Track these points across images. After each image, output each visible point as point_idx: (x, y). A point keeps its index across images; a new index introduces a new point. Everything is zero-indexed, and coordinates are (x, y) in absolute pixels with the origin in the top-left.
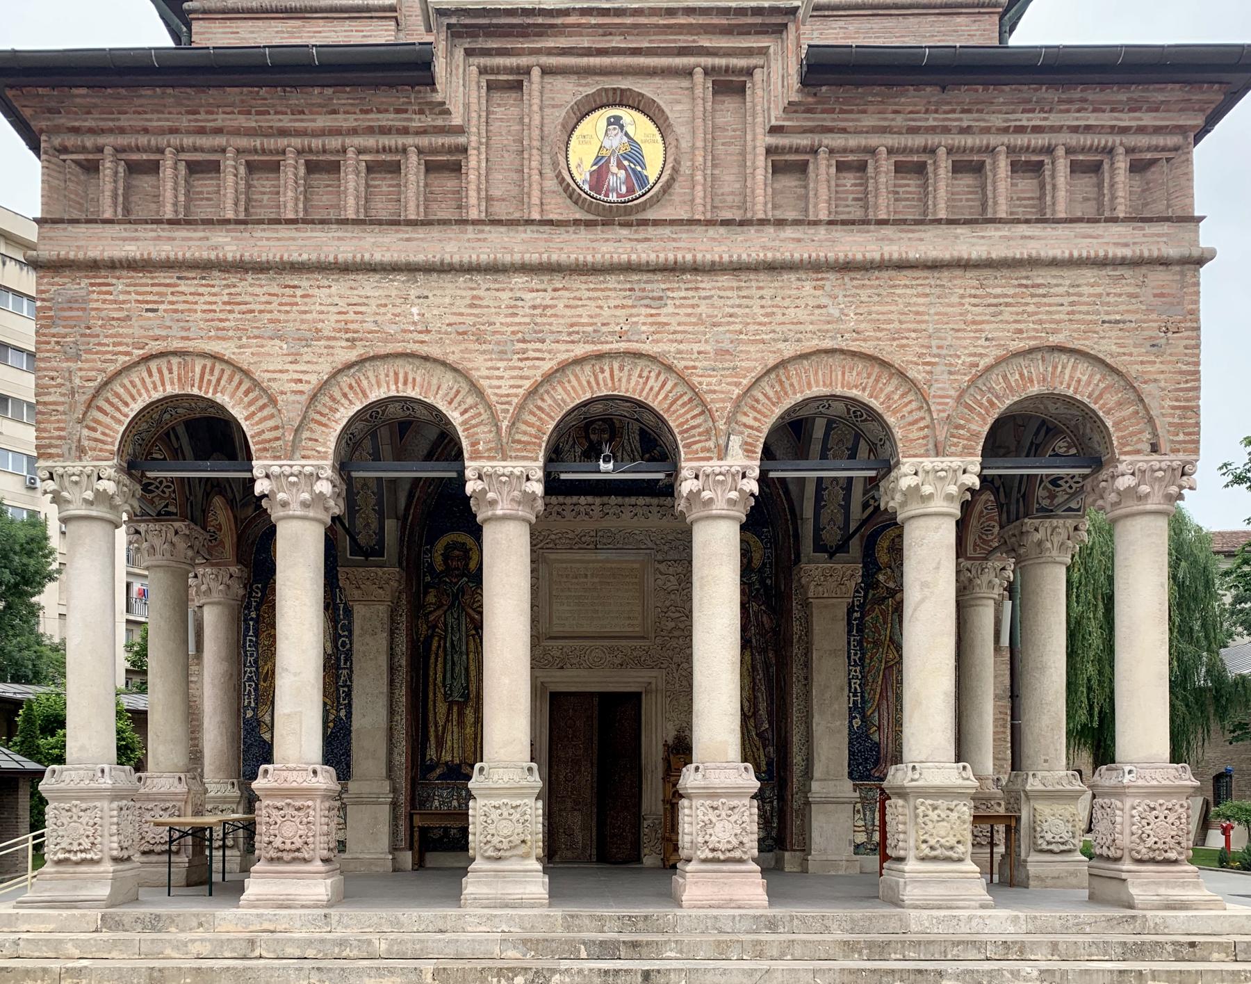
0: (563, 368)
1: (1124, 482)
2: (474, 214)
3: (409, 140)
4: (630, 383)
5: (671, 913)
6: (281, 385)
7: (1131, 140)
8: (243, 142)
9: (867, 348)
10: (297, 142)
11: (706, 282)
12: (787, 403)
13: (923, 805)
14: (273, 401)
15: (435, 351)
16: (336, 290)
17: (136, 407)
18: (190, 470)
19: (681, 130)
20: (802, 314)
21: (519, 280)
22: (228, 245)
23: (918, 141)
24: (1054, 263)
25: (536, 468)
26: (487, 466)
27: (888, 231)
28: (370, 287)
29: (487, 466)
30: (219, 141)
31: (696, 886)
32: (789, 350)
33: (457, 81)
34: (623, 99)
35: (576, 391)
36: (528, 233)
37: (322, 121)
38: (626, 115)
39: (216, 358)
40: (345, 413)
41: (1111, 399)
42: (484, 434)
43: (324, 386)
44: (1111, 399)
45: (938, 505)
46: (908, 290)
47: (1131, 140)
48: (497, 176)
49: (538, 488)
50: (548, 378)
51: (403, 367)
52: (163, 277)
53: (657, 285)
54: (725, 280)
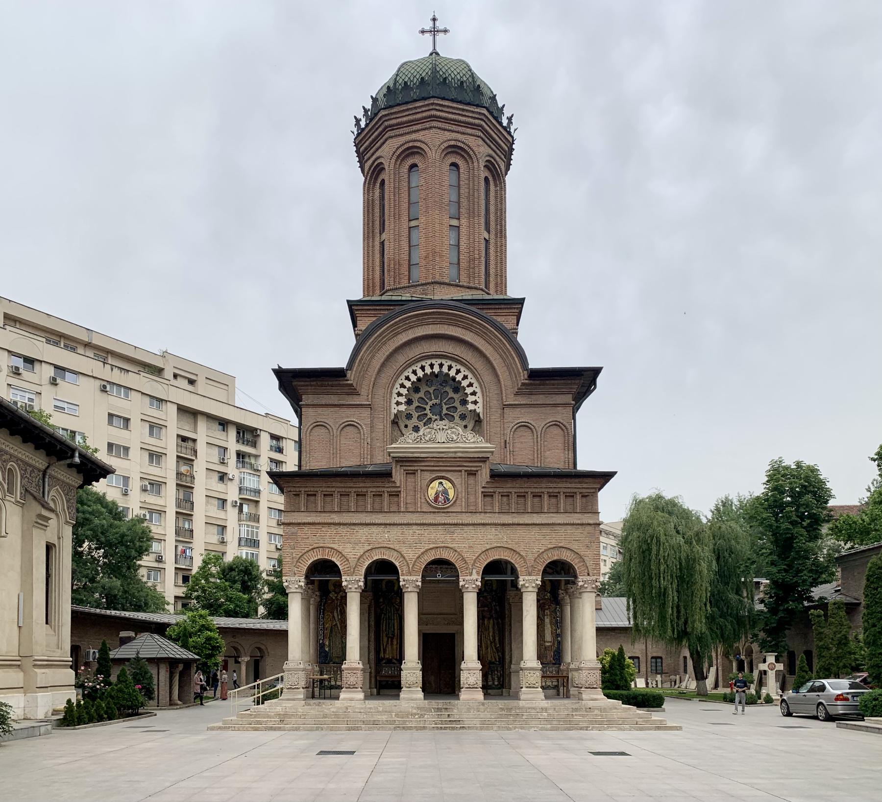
0: (427, 551)
1: (580, 584)
2: (402, 509)
3: (385, 489)
4: (445, 555)
5: (456, 702)
6: (350, 556)
7: (581, 491)
8: (340, 490)
9: (510, 546)
10: (354, 490)
11: (466, 528)
12: (488, 561)
13: (527, 672)
14: (348, 560)
15: (392, 546)
16: (366, 530)
17: (310, 562)
18: (324, 578)
19: (458, 486)
20: (492, 537)
21: (414, 527)
22: (336, 518)
23: (523, 490)
24: (559, 524)
25: (419, 578)
26: (406, 578)
27: (515, 515)
28: (374, 529)
29: (406, 578)
30: (333, 489)
31: (464, 695)
32: (488, 547)
33: (398, 475)
34: (443, 478)
35: (431, 557)
36: (417, 515)
37: (362, 485)
38: (444, 481)
39: (332, 548)
40: (367, 563)
41: (577, 561)
42: (405, 569)
43: (361, 556)
44: (577, 561)
45: (530, 589)
46: (521, 531)
47: (581, 491)
48: (409, 497)
49: (420, 584)
50: (422, 554)
51: (383, 550)
52: (317, 527)
53: (452, 529)
54: (471, 527)
